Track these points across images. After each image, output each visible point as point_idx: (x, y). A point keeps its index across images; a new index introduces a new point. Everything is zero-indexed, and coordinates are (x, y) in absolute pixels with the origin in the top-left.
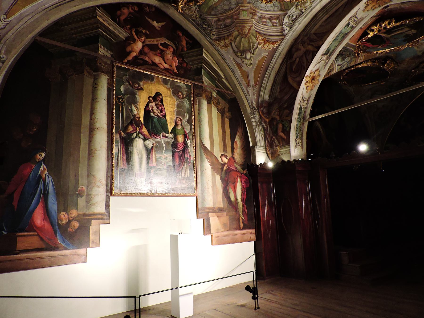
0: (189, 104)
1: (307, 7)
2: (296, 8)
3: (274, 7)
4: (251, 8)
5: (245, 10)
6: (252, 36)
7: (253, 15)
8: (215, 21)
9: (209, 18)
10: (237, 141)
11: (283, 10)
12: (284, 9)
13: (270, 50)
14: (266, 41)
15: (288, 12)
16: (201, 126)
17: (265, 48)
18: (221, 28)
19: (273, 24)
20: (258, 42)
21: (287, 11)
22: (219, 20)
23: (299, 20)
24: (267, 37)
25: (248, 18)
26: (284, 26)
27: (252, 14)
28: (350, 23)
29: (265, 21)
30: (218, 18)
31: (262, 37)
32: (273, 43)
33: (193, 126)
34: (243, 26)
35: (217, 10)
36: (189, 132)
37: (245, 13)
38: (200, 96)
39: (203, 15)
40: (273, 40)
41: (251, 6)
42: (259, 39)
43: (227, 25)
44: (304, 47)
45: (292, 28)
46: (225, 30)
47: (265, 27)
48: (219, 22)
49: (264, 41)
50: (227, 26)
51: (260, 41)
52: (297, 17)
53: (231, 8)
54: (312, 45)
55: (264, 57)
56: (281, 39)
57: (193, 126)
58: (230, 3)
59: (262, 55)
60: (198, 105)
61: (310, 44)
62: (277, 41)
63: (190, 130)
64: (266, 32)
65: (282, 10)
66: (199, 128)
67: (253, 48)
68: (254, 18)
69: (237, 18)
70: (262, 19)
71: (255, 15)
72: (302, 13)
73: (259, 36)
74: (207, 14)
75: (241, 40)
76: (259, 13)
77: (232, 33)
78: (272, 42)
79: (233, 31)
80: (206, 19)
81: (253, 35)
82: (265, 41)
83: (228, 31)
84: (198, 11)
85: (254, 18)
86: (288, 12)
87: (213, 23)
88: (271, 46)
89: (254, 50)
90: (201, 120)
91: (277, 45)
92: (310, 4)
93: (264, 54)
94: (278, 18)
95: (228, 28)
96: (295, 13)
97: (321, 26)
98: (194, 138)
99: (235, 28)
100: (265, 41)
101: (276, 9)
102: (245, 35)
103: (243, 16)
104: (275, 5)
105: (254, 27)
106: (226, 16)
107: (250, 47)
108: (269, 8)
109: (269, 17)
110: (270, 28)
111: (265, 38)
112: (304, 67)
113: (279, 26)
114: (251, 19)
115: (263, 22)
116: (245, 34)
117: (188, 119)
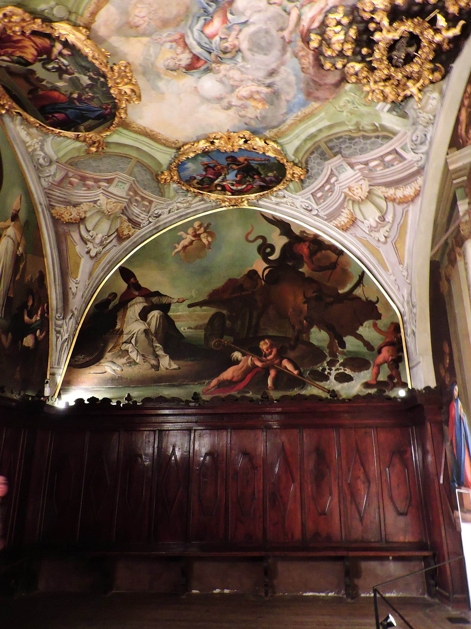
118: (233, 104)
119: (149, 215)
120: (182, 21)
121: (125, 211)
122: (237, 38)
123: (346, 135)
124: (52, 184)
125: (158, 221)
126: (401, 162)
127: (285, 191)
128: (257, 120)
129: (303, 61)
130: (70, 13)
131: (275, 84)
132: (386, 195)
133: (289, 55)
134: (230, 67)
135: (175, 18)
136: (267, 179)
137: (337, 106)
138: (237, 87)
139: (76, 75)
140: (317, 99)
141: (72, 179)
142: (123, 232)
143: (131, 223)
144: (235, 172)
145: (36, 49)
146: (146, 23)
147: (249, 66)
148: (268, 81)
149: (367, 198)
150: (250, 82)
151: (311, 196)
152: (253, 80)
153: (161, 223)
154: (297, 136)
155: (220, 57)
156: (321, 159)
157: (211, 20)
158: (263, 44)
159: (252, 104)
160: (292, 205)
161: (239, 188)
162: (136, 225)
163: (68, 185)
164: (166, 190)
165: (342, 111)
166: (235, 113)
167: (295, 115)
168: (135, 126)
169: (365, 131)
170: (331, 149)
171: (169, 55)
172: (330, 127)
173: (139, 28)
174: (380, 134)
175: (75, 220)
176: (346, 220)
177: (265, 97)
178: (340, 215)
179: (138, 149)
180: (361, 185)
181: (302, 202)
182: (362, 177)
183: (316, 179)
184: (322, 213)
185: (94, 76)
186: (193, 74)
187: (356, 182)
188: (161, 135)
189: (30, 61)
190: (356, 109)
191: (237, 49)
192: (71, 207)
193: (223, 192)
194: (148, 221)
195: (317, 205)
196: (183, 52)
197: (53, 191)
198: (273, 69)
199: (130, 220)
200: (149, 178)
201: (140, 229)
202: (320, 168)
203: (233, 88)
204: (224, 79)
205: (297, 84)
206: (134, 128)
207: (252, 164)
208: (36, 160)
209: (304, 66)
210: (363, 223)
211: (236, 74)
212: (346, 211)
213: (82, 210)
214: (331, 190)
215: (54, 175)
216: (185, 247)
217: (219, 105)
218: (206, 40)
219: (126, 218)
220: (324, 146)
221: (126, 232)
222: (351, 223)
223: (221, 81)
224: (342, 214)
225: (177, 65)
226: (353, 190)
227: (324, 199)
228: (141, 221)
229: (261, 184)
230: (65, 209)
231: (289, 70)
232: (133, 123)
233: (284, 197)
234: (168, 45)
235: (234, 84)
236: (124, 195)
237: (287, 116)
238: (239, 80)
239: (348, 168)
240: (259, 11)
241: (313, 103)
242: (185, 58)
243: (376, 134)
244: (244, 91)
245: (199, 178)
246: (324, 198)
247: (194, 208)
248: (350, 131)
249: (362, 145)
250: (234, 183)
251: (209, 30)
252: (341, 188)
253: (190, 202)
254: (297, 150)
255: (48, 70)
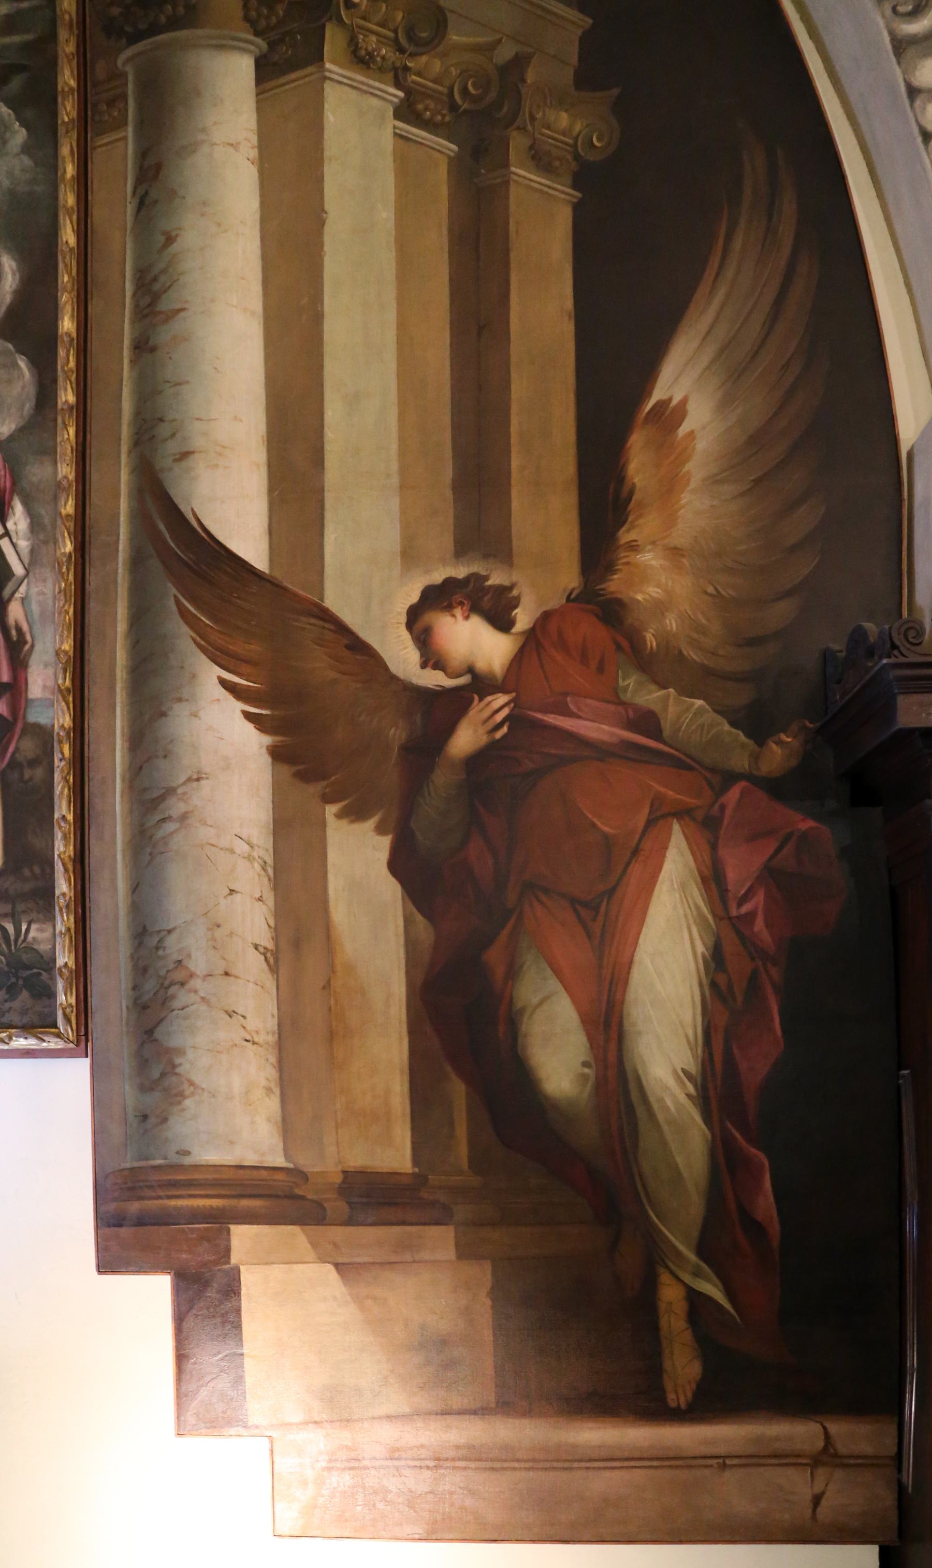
0: (26, 149)
10: (684, 402)
16: (163, 335)
33: (67, 360)
36: (21, 430)
38: (175, 24)
57: (67, 360)
60: (140, 124)
63: (29, 407)
66: (132, 362)
90: (164, 271)
98: (66, 470)
117: (8, 299)
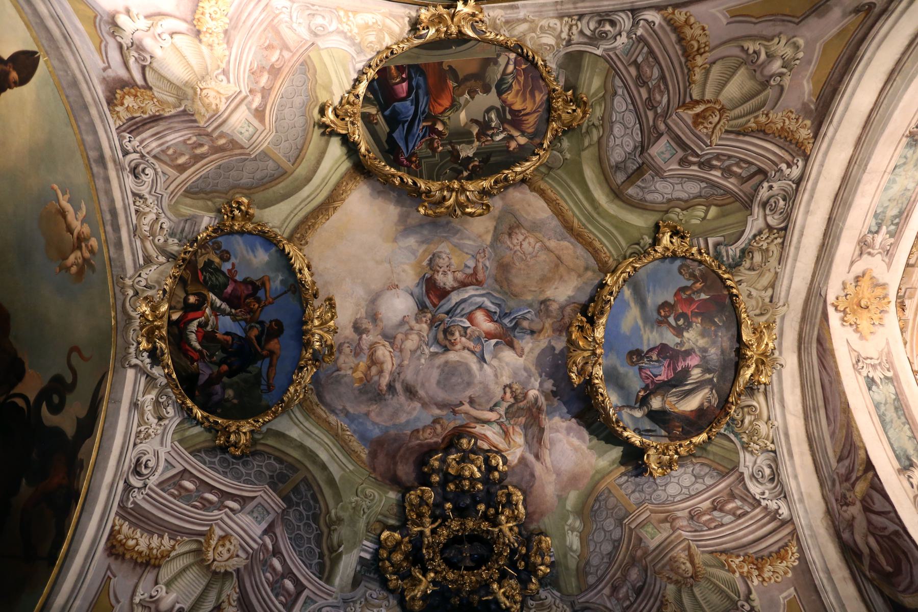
1: (768, 435)
2: (748, 451)
3: (701, 481)
4: (652, 512)
5: (645, 522)
6: (709, 569)
7: (671, 523)
8: (608, 597)
9: (591, 598)
11: (728, 473)
12: (727, 471)
13: (790, 575)
14: (758, 562)
15: (740, 470)
17: (770, 579)
18: (632, 604)
19: (734, 514)
20: (737, 575)
21: (738, 470)
22: (615, 589)
23: (786, 472)
24: (751, 551)
25: (665, 535)
26: (764, 503)
27: (668, 522)
28: (871, 376)
29: (711, 519)
30: (610, 585)
31: (738, 556)
32: (780, 554)
34: (670, 560)
35: (593, 566)
37: (650, 529)
39: (576, 603)
40: (774, 548)
41: (650, 507)
42: (734, 566)
43: (638, 585)
44: (854, 504)
45: (789, 496)
46: (643, 601)
47: (723, 532)
48: (618, 592)
49: (754, 564)
50: (641, 588)
51: (741, 571)
52: (774, 467)
53: (615, 541)
54: (858, 479)
55: (790, 603)
56: (789, 534)
58: (605, 531)
59: (782, 600)
61: (853, 485)
62: (787, 545)
64: (735, 540)
65: (723, 475)
67: (739, 597)
68: (677, 526)
69: (646, 554)
70: (699, 517)
71: (674, 520)
72: (775, 452)
73: (730, 560)
74: (582, 592)
75: (694, 596)
76: (679, 511)
77: (664, 597)
78: (774, 555)
79: (660, 587)
80: (587, 605)
81: (710, 566)
82: (756, 562)
83: (650, 598)
84: (561, 600)
85: (678, 529)
86: (740, 470)
87: (609, 605)
88: (781, 566)
89: (748, 599)
91: (797, 555)
92: (768, 426)
93: (785, 594)
94: (732, 496)
95: (644, 591)
96: (758, 461)
97: (832, 435)
99: (658, 579)
100: (756, 562)
101: (709, 481)
102: (692, 577)
103: (652, 538)
104: (698, 474)
105: (698, 546)
106: (620, 566)
107: (728, 597)
108: (691, 489)
109: (711, 506)
110: (737, 526)
111: (746, 554)
112: (896, 533)
113: (753, 510)
114: (674, 532)
115: (705, 524)
116: (690, 575)
118: (364, 336)
119: (148, 157)
120: (501, 287)
121: (186, 118)
122: (464, 348)
123: (320, 508)
124: (277, 16)
125: (120, 167)
126: (284, 605)
127: (177, 420)
128: (334, 369)
129: (429, 431)
130: (550, 169)
131: (393, 396)
132: (224, 605)
133: (437, 412)
134: (423, 336)
135: (507, 279)
136: (218, 388)
137: (364, 485)
138: (392, 344)
139: (476, 144)
140: (373, 455)
141: (278, 52)
142: (136, 96)
143: (150, 117)
144: (240, 333)
145: (520, 111)
146: (511, 246)
147: (423, 361)
148: (398, 386)
149: (215, 573)
150: (399, 362)
151: (179, 468)
152: (400, 366)
153: (112, 174)
154: (309, 434)
155: (440, 324)
156: (271, 477)
157: (492, 320)
158: (454, 380)
159: (361, 364)
160: (142, 436)
161: (193, 337)
162: (135, 126)
163: (268, 42)
164: (201, 203)
165: (357, 495)
166: (346, 338)
167: (345, 426)
168: (349, 187)
169: (329, 534)
170: (296, 490)
171: (455, 261)
172: (331, 482)
173: (507, 236)
174: (326, 559)
175: (199, 20)
176: (142, 546)
177: (373, 381)
178: (151, 533)
179: (308, 180)
180: (238, 556)
181: (157, 454)
182: (251, 551)
183: (225, 474)
184: (140, 497)
185: (472, 165)
186: (420, 286)
187: (241, 545)
188: (324, 221)
189: (504, 96)
190: (362, 512)
191: (449, 346)
192: (227, 27)
193: (182, 305)
194: (132, 151)
195: (160, 485)
196: (455, 279)
197: (264, 10)
198: (417, 392)
199: (155, 119)
200: (242, 181)
201: (117, 129)
202: (253, 479)
203: (390, 338)
204: (407, 327)
205: (394, 425)
206: (347, 184)
207: (259, 363)
208: (323, 14)
209: (421, 433)
210: (153, 584)
211: (412, 343)
212: (167, 542)
213: (216, 41)
214: (207, 505)
215: (291, 28)
216: (63, 213)
217: (364, 315)
218: (467, 310)
219: (167, 114)
220: (299, 476)
221: (129, 101)
222: (139, 560)
223: (403, 322)
224: (156, 536)
225: (438, 268)
226: (223, 546)
227: (180, 494)
228: (138, 138)
229: (201, 377)
230: (225, 12)
231: (415, 414)
232: (356, 186)
233: (160, 419)
234: (471, 263)
235: (396, 340)
236: (225, 129)
237: (342, 415)
238: (403, 347)
239: (264, 525)
240: (496, 376)
241: (367, 452)
242: (446, 280)
243: (326, 552)
244: (383, 352)
245: (225, 267)
246: (185, 496)
247: (131, 244)
248: (328, 512)
249: (305, 536)
250: (209, 328)
251: (480, 316)
252: (219, 521)
253: (151, 238)
254: (280, 435)
255: (488, 111)
